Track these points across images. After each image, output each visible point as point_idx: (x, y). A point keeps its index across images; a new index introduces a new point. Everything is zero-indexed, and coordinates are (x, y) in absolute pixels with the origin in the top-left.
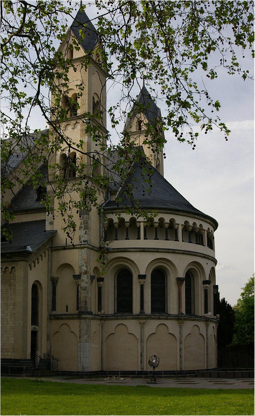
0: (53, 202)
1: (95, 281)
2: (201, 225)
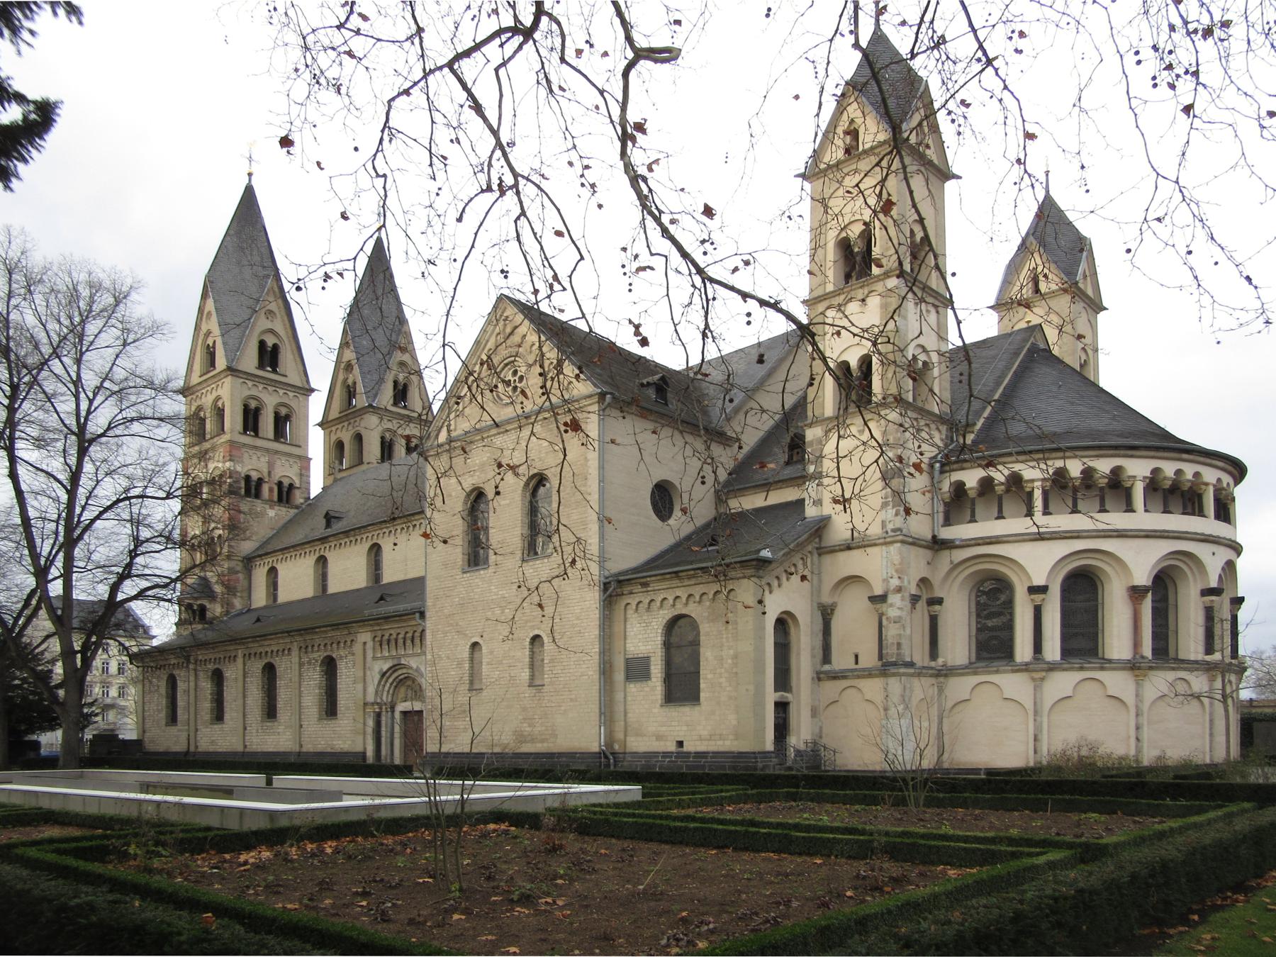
1: (921, 605)
2: (1197, 475)
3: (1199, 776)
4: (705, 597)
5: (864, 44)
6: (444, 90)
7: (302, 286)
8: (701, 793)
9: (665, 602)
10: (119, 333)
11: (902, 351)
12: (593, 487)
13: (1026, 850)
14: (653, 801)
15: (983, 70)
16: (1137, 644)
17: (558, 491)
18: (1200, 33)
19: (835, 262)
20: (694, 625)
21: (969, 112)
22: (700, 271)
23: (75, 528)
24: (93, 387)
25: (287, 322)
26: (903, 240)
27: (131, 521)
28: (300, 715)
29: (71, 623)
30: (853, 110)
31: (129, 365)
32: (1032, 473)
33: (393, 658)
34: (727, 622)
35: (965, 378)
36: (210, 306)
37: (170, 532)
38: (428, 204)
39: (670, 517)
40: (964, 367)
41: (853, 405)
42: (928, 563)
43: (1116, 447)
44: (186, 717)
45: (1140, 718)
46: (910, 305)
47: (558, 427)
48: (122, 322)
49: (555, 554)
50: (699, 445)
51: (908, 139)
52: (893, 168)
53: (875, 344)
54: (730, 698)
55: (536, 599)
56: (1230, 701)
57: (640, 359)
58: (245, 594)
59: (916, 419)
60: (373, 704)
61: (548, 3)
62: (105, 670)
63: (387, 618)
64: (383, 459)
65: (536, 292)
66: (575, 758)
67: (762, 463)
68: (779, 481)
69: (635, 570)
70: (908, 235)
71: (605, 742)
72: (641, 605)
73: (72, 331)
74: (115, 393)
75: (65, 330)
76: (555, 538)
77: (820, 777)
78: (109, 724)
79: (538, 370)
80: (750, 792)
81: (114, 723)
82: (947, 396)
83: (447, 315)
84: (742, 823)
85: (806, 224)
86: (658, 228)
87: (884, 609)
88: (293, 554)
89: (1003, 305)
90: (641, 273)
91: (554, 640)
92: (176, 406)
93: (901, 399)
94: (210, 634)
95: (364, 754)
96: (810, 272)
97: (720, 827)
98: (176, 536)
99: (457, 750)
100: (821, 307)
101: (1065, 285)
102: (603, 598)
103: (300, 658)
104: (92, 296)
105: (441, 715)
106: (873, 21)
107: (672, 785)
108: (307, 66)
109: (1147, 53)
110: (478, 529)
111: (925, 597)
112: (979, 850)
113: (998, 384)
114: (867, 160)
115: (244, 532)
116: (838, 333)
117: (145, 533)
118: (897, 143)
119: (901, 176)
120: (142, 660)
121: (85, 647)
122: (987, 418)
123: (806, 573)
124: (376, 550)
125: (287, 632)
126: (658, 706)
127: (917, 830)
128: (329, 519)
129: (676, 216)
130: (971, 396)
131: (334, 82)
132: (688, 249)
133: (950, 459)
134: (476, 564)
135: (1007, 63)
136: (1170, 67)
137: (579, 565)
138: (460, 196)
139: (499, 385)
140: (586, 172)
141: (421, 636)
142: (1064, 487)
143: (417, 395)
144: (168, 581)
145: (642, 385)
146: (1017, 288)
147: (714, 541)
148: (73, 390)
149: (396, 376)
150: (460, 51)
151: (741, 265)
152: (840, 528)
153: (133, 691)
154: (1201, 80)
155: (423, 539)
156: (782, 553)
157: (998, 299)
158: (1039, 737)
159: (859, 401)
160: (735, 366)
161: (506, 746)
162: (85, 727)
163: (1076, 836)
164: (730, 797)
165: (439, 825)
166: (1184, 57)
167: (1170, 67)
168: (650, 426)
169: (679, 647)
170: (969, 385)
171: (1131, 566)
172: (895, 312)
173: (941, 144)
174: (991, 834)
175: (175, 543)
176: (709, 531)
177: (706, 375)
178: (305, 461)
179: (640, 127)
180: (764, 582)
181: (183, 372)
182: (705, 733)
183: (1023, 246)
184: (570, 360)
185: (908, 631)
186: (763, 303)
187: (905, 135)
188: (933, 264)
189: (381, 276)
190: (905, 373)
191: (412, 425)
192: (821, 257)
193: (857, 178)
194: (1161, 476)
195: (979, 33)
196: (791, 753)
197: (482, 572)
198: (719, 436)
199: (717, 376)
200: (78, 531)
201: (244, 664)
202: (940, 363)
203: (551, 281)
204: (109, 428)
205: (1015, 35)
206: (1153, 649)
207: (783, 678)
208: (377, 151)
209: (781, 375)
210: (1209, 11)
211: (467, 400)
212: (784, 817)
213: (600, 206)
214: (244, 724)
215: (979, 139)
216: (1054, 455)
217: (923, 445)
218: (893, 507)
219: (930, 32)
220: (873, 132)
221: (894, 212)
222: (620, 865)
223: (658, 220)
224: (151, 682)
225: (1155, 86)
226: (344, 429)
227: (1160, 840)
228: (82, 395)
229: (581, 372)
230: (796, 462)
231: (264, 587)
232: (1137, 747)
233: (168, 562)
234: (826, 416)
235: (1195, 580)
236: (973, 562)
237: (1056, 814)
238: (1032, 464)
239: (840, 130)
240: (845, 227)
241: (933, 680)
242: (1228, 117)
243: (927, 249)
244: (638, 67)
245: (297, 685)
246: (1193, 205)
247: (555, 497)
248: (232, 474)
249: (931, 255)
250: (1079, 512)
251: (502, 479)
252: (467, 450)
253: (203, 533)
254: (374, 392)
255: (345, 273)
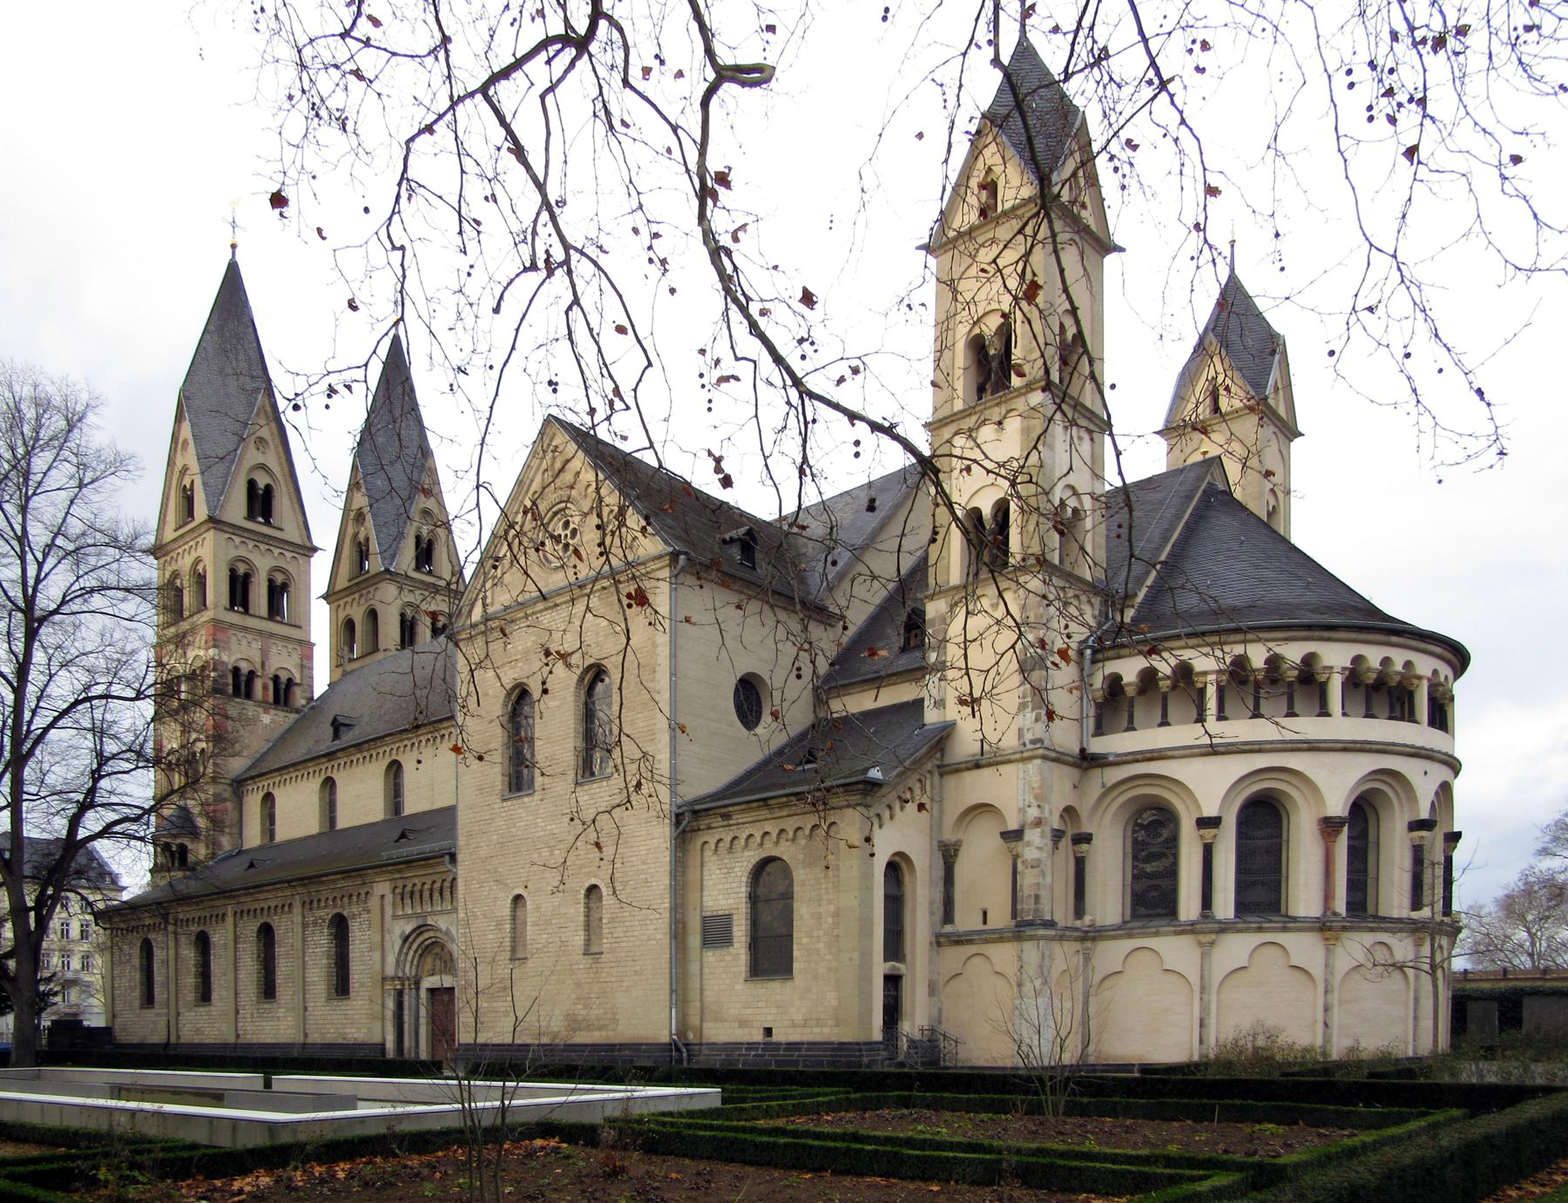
1: (1065, 842)
3: (1399, 1073)
4: (800, 833)
5: (1005, 59)
6: (476, 127)
7: (300, 403)
8: (792, 1098)
9: (752, 840)
10: (74, 470)
11: (1047, 494)
12: (663, 682)
13: (1187, 1172)
14: (735, 1109)
15: (1155, 96)
16: (1328, 896)
17: (620, 689)
18: (1430, 43)
19: (965, 369)
20: (786, 872)
21: (1137, 157)
22: (797, 383)
23: (24, 740)
24: (42, 544)
25: (282, 455)
26: (1050, 339)
27: (93, 730)
28: (304, 994)
29: (21, 870)
30: (991, 155)
31: (87, 515)
32: (1206, 663)
33: (417, 916)
34: (827, 868)
35: (1124, 531)
36: (186, 431)
37: (142, 746)
38: (458, 288)
39: (757, 724)
40: (1123, 516)
41: (985, 569)
43: (1309, 627)
44: (165, 996)
45: (1329, 996)
46: (1058, 429)
47: (619, 600)
48: (76, 455)
49: (616, 775)
50: (795, 626)
51: (1058, 195)
52: (1040, 236)
53: (1013, 484)
54: (830, 969)
55: (592, 837)
56: (1439, 973)
57: (722, 506)
58: (235, 831)
59: (1063, 589)
60: (393, 979)
61: (607, 3)
62: (65, 934)
63: (409, 863)
64: (403, 645)
65: (592, 411)
66: (639, 1050)
67: (871, 649)
68: (893, 674)
69: (715, 796)
70: (1057, 332)
71: (677, 1029)
72: (721, 844)
73: (14, 467)
74: (69, 553)
75: (6, 466)
76: (616, 753)
77: (938, 1076)
78: (70, 1006)
79: (595, 520)
80: (853, 1096)
81: (77, 1005)
82: (1101, 556)
83: (482, 445)
84: (843, 1137)
85: (930, 316)
86: (745, 322)
87: (1020, 849)
88: (293, 775)
89: (1173, 430)
90: (724, 385)
91: (614, 892)
92: (144, 571)
93: (1045, 560)
94: (192, 883)
95: (383, 1045)
96: (934, 384)
97: (816, 1143)
98: (149, 751)
99: (496, 1041)
100: (947, 433)
101: (1252, 402)
102: (674, 835)
103: (304, 917)
104: (38, 418)
105: (477, 993)
106: (1018, 25)
107: (758, 1087)
108: (304, 92)
109: (1362, 73)
110: (521, 740)
111: (1069, 833)
112: (1130, 1172)
113: (1165, 540)
114: (1008, 225)
115: (233, 745)
116: (968, 469)
117: (111, 747)
118: (1045, 202)
119: (1050, 248)
120: (110, 920)
121: (40, 902)
122: (1150, 587)
123: (925, 800)
124: (395, 769)
125: (288, 882)
126: (742, 980)
127: (1056, 1146)
128: (338, 727)
129: (767, 305)
130: (1132, 556)
131: (338, 115)
132: (783, 351)
133: (1104, 645)
134: (519, 789)
135: (1185, 87)
136: (1390, 93)
137: (645, 790)
138: (497, 277)
139: (547, 542)
140: (655, 242)
141: (452, 887)
142: (1244, 682)
143: (445, 555)
144: (140, 812)
145: (724, 541)
146: (1191, 406)
147: (811, 757)
148: (18, 550)
149: (419, 529)
150: (496, 70)
151: (848, 373)
152: (967, 742)
153: (100, 962)
154: (1429, 111)
155: (453, 755)
156: (895, 773)
157: (1167, 421)
158: (1206, 1022)
159: (993, 563)
160: (839, 515)
161: (556, 1035)
162: (42, 1010)
163: (1248, 1154)
164: (828, 1103)
165: (475, 1141)
166: (1408, 79)
167: (1390, 93)
168: (734, 598)
169: (767, 901)
170: (1130, 541)
171: (1323, 789)
172: (1039, 439)
173: (1100, 201)
174: (1145, 1152)
175: (148, 761)
176: (805, 743)
177: (804, 528)
178: (307, 647)
179: (723, 179)
180: (872, 812)
181: (154, 524)
182: (799, 1017)
183: (1200, 348)
184: (635, 507)
185: (1048, 879)
186: (875, 427)
187: (1056, 190)
188: (1087, 372)
189: (399, 390)
190: (1050, 524)
191: (438, 597)
192: (948, 362)
193: (995, 250)
194: (1364, 667)
195: (1150, 43)
196: (904, 1044)
197: (526, 799)
198: (817, 612)
199: (817, 529)
200: (28, 745)
201: (235, 926)
202: (1094, 510)
203: (611, 396)
204: (63, 602)
205: (1197, 47)
206: (1348, 903)
207: (895, 944)
208: (393, 213)
209: (895, 528)
210: (1441, 12)
211: (507, 562)
212: (894, 1129)
213: (673, 291)
214: (236, 1005)
215: (1148, 195)
216: (1232, 638)
217: (1070, 624)
218: (1033, 710)
219: (1090, 41)
220: (1016, 187)
221: (1040, 299)
222: (694, 1193)
223: (744, 310)
224: (121, 950)
225: (1371, 119)
226: (355, 604)
227: (1349, 1158)
228: (29, 557)
229: (649, 524)
230: (914, 648)
231: (259, 821)
232: (1324, 1035)
233: (139, 787)
234: (951, 584)
235: (1402, 807)
236: (1124, 787)
237: (1224, 1124)
238: (1205, 650)
239: (974, 183)
240: (979, 320)
242: (1460, 163)
243: (1081, 350)
244: (720, 92)
245: (300, 952)
246: (1413, 289)
247: (616, 698)
248: (216, 664)
249: (1085, 359)
250: (1262, 716)
251: (551, 672)
252: (507, 631)
253: (183, 747)
254: (391, 551)
255: (354, 385)
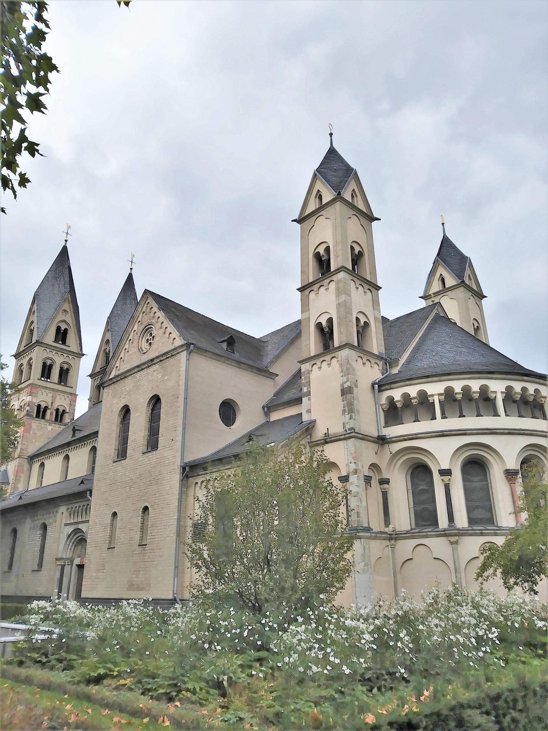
0: (310, 385)
2: (537, 391)
42: (376, 453)
241: (387, 543)
